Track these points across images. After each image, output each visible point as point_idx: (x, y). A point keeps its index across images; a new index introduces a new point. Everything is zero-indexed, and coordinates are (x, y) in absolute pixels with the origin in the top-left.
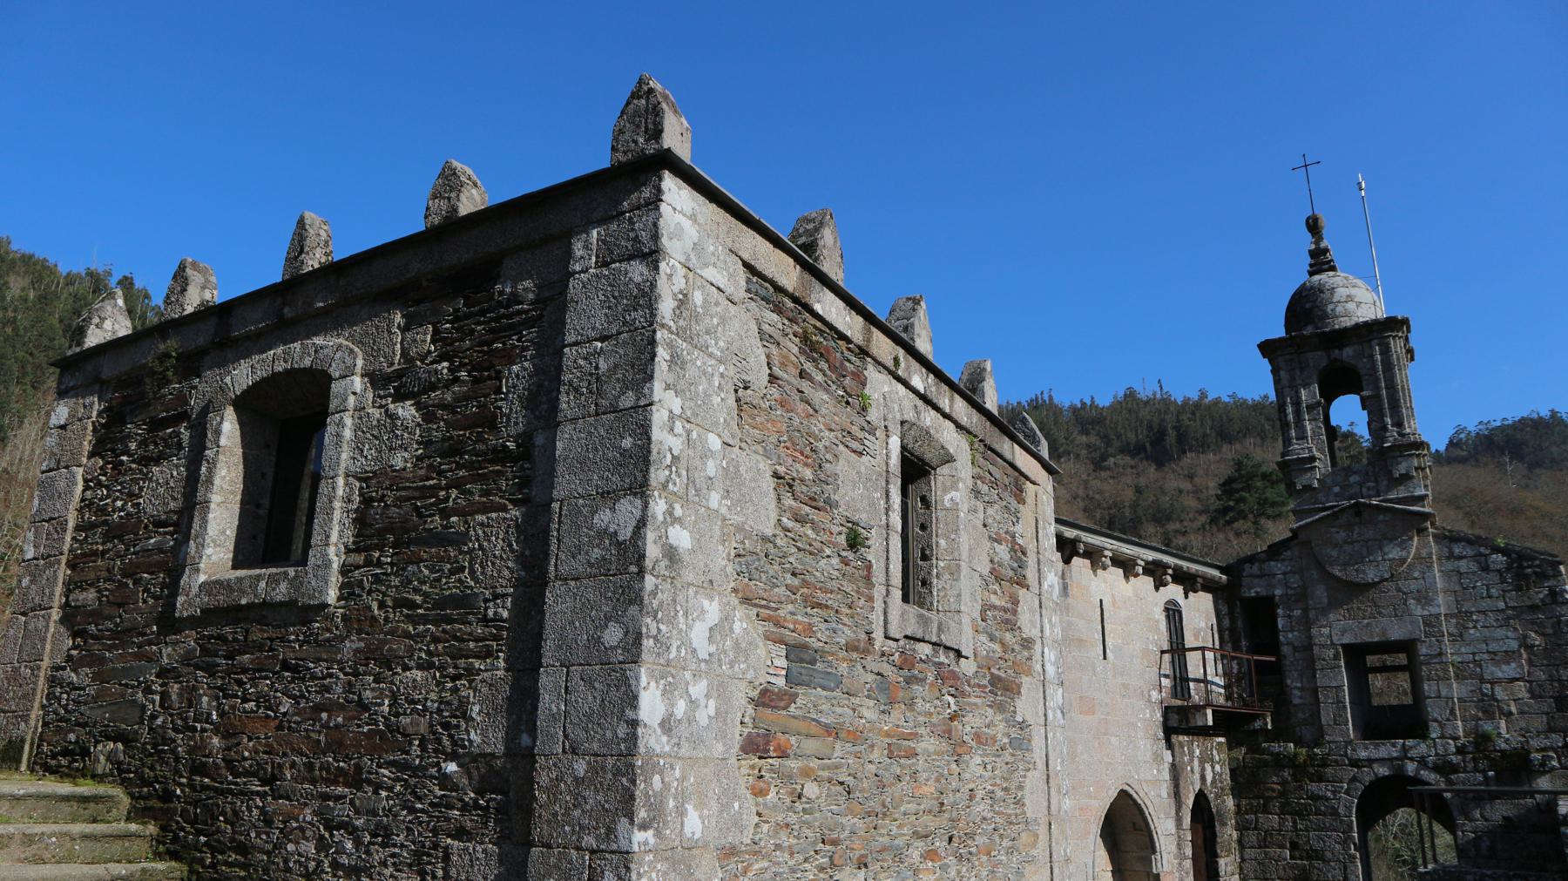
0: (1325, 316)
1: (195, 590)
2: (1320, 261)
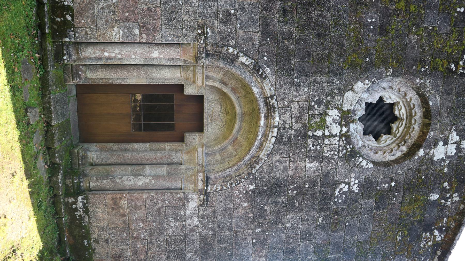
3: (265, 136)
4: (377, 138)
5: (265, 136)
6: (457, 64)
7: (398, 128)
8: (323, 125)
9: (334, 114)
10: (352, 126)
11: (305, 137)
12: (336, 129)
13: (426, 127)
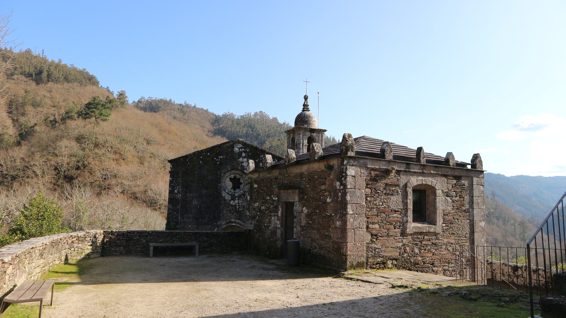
0: (310, 124)
1: (411, 228)
2: (306, 107)
3: (238, 223)
4: (242, 183)
5: (238, 223)
6: (218, 161)
7: (238, 177)
8: (235, 206)
9: (232, 202)
10: (236, 195)
11: (238, 211)
12: (237, 201)
13: (237, 170)
